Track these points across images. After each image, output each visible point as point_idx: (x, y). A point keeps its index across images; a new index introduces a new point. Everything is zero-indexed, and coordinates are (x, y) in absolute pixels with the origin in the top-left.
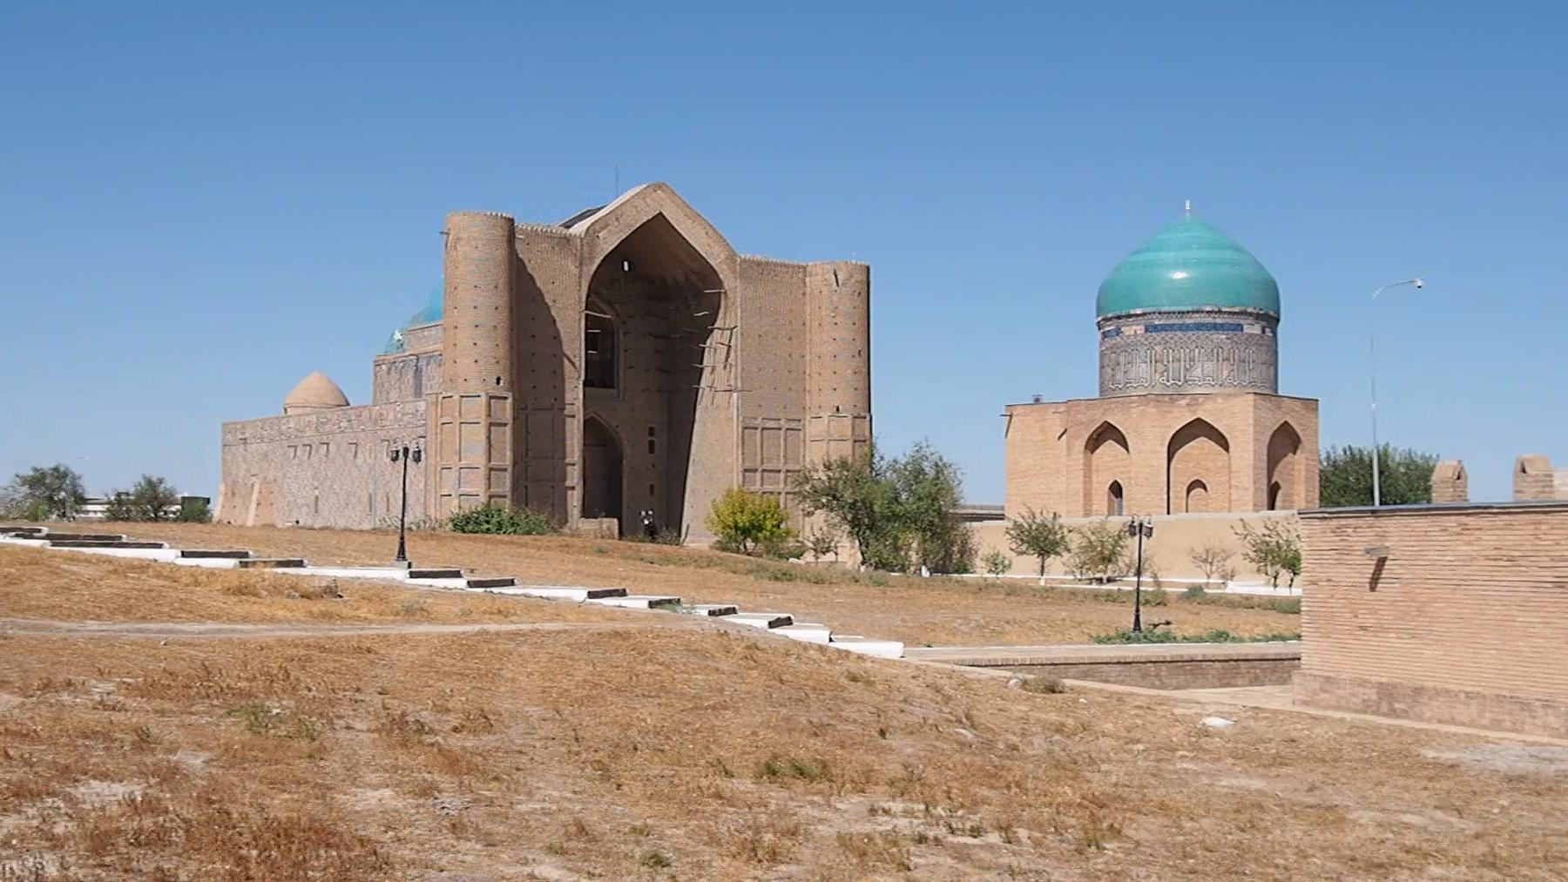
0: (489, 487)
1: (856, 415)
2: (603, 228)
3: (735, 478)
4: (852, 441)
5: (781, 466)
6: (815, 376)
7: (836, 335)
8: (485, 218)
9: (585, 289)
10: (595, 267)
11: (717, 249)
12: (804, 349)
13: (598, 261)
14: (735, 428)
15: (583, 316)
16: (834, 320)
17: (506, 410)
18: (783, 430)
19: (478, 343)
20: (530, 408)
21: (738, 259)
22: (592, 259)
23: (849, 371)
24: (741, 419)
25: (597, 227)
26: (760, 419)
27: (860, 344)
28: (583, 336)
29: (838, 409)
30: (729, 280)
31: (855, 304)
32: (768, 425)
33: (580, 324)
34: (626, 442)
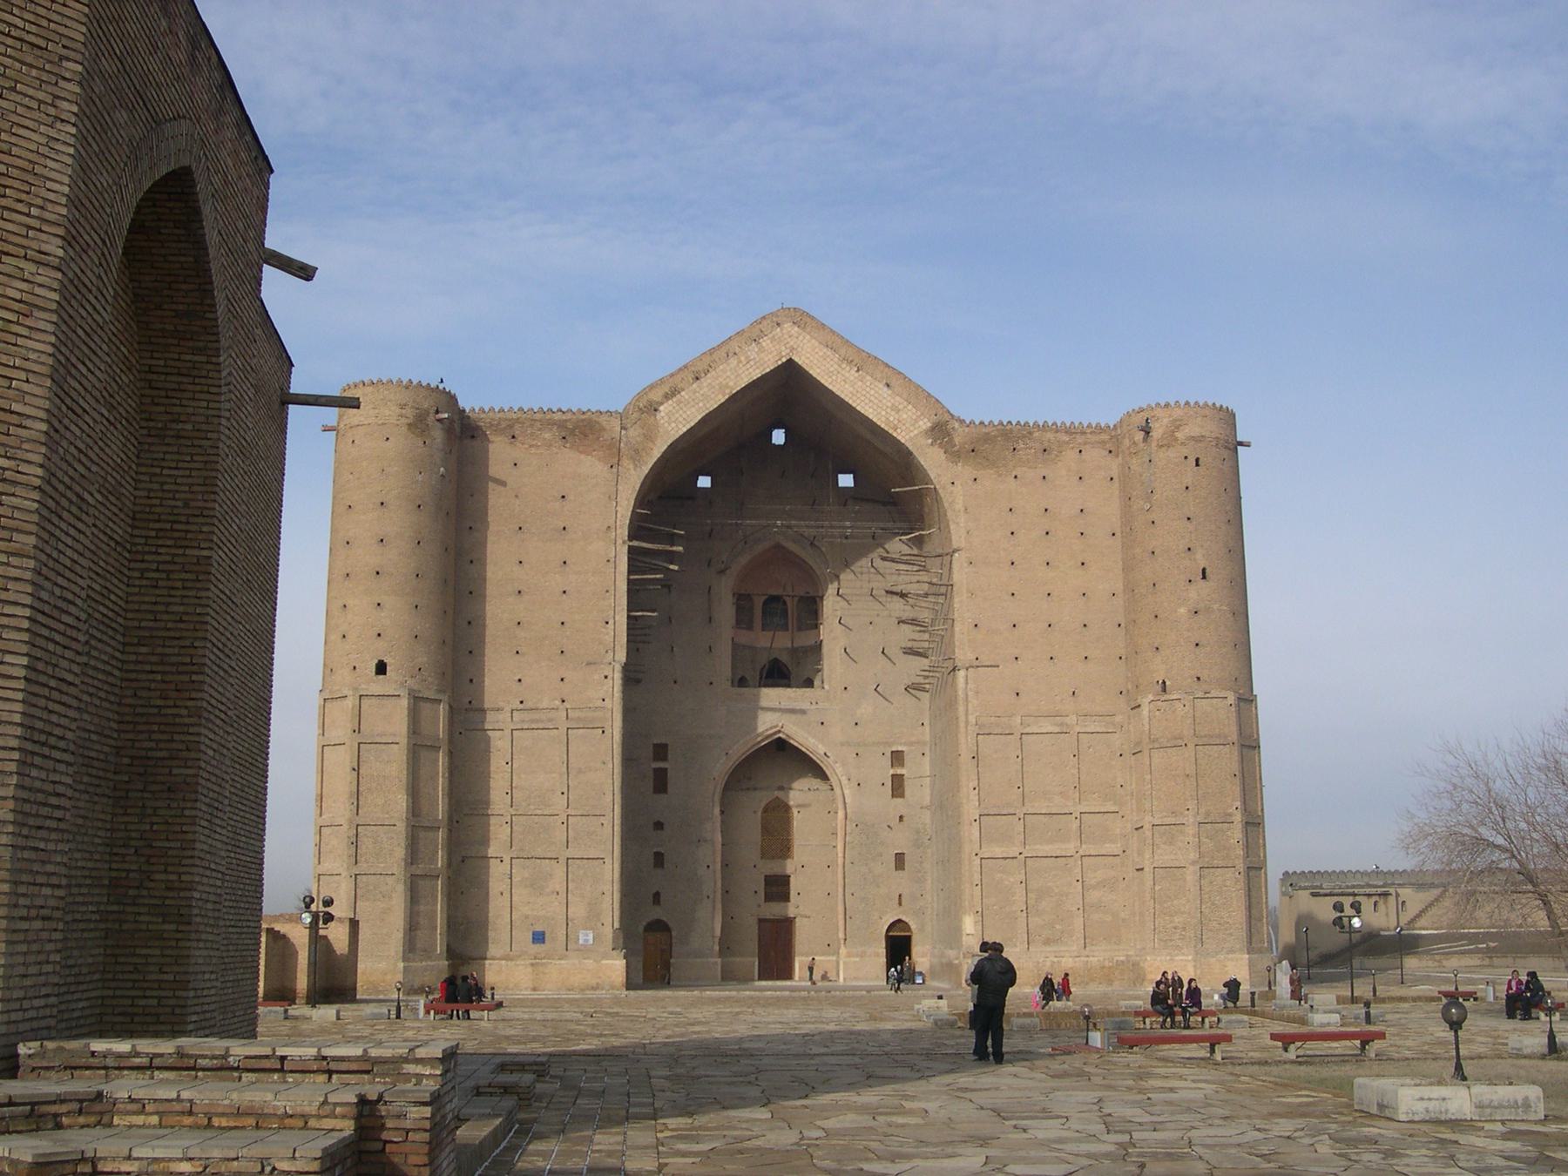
2: (667, 397)
11: (909, 413)
23: (1182, 610)
24: (972, 719)
28: (623, 587)
31: (1188, 481)
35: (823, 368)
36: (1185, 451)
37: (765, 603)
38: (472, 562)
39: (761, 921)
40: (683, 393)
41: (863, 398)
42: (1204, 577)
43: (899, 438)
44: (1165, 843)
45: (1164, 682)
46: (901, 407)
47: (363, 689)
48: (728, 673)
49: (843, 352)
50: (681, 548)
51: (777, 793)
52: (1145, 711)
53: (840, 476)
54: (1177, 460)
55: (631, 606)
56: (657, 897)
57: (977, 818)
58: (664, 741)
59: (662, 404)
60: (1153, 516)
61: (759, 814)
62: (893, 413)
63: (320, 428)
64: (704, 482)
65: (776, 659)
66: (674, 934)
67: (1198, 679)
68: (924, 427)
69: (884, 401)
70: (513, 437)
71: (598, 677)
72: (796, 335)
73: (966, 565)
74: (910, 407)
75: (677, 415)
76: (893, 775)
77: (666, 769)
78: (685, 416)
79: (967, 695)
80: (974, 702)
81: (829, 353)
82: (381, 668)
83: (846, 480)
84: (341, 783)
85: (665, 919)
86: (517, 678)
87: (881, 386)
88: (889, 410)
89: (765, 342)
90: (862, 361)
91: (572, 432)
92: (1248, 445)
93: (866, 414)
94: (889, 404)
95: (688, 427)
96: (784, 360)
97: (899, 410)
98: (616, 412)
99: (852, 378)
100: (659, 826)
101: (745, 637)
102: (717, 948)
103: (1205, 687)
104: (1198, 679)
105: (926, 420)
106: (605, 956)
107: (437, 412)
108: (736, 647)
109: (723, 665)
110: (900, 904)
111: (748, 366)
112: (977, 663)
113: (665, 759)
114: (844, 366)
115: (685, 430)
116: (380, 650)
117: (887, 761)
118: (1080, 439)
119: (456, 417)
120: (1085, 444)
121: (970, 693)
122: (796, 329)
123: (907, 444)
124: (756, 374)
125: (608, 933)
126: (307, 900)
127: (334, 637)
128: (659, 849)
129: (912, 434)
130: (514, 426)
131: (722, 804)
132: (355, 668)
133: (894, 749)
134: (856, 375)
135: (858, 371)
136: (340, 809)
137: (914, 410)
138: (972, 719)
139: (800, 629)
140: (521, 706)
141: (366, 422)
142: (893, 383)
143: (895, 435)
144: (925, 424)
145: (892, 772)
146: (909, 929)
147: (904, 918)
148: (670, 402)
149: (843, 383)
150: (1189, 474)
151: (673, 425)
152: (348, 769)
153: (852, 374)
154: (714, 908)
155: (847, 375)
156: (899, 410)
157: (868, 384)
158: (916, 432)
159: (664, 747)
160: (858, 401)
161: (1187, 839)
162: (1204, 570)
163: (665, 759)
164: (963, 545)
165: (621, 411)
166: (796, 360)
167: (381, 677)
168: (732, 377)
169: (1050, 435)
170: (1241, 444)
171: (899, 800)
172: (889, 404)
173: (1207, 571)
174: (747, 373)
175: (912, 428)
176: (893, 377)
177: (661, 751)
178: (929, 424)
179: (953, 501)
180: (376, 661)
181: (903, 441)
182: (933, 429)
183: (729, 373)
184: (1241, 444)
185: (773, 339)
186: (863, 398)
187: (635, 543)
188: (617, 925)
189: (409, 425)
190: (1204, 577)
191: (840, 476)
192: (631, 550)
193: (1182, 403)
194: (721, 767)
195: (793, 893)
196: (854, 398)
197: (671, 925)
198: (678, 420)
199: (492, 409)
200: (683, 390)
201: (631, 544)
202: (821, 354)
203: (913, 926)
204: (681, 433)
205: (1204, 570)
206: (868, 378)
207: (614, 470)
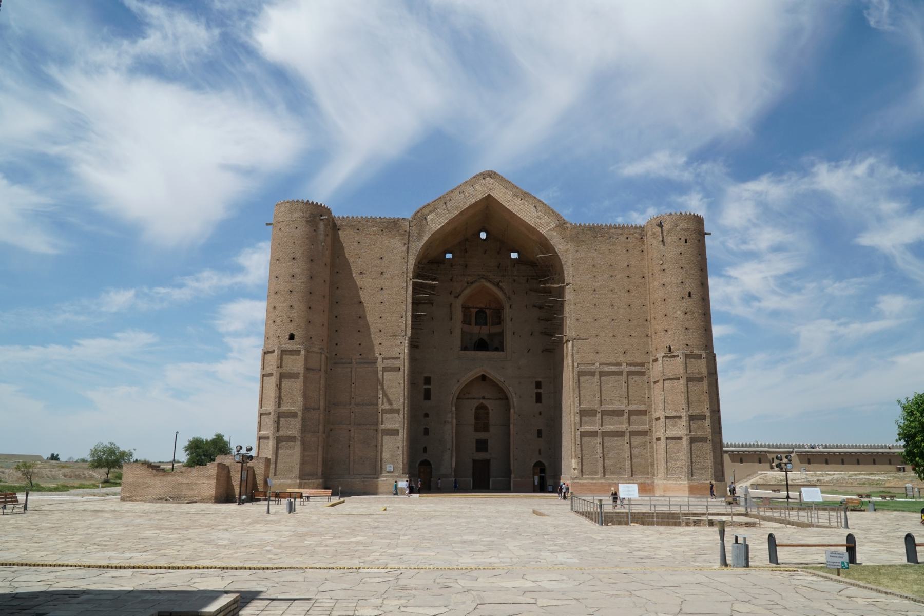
0: (278, 431)
1: (688, 352)
2: (431, 212)
3: (572, 419)
4: (685, 378)
5: (623, 407)
6: (653, 321)
7: (665, 280)
8: (288, 204)
9: (412, 261)
10: (423, 244)
12: (646, 299)
13: (425, 239)
14: (571, 374)
15: (411, 283)
16: (663, 267)
17: (297, 364)
18: (625, 374)
19: (277, 305)
21: (568, 225)
22: (420, 237)
24: (576, 364)
25: (426, 211)
26: (597, 364)
27: (691, 285)
28: (410, 300)
29: (670, 349)
30: (560, 246)
32: (607, 369)
33: (406, 291)
35: (505, 198)
36: (680, 236)
37: (477, 313)
38: (338, 288)
39: (474, 461)
40: (438, 210)
41: (523, 213)
42: (690, 296)
43: (541, 231)
44: (672, 425)
45: (670, 347)
46: (541, 217)
47: (283, 347)
48: (459, 343)
49: (514, 191)
50: (437, 282)
51: (482, 401)
52: (660, 360)
53: (512, 254)
54: (675, 240)
55: (414, 310)
56: (425, 449)
57: (578, 411)
58: (429, 375)
59: (428, 215)
60: (664, 267)
61: (474, 410)
62: (538, 220)
63: (265, 224)
64: (449, 256)
65: (481, 338)
66: (433, 466)
67: (687, 345)
68: (552, 226)
69: (533, 214)
70: (358, 230)
71: (398, 342)
72: (492, 183)
73: (572, 291)
74: (546, 217)
75: (436, 220)
76: (536, 393)
77: (430, 389)
78: (439, 220)
79: (573, 353)
80: (576, 356)
81: (507, 192)
82: (292, 337)
83: (514, 255)
84: (271, 392)
85: (428, 459)
86: (359, 343)
87: (532, 207)
88: (536, 218)
89: (478, 187)
91: (386, 228)
92: (709, 234)
93: (525, 220)
94: (536, 216)
95: (441, 226)
96: (486, 195)
97: (541, 218)
98: (407, 219)
99: (518, 203)
100: (426, 415)
102: (453, 474)
103: (691, 349)
104: (687, 345)
105: (553, 223)
106: (399, 477)
107: (321, 216)
109: (456, 339)
110: (540, 454)
111: (469, 197)
112: (577, 338)
113: (430, 384)
114: (514, 197)
115: (439, 227)
116: (291, 328)
117: (534, 384)
118: (626, 231)
119: (331, 220)
120: (630, 234)
121: (574, 352)
122: (492, 180)
123: (545, 234)
124: (473, 201)
125: (401, 465)
126: (239, 447)
127: (270, 322)
128: (427, 426)
129: (547, 230)
130: (358, 225)
131: (456, 405)
132: (279, 337)
133: (537, 380)
134: (520, 202)
135: (521, 200)
136: (270, 406)
137: (548, 218)
138: (576, 364)
139: (492, 325)
140: (360, 357)
141: (286, 219)
142: (538, 206)
143: (539, 230)
144: (553, 225)
145: (536, 391)
146: (544, 466)
147: (541, 460)
148: (432, 214)
149: (514, 206)
150: (683, 247)
151: (434, 225)
152: (275, 385)
153: (518, 201)
154: (452, 454)
155: (516, 202)
156: (541, 218)
157: (526, 206)
158: (548, 228)
159: (430, 378)
160: (521, 214)
161: (683, 423)
162: (690, 293)
163: (430, 384)
167: (292, 341)
168: (462, 203)
169: (613, 230)
171: (539, 405)
172: (536, 216)
173: (692, 293)
174: (469, 201)
175: (547, 227)
177: (428, 380)
178: (555, 225)
179: (567, 261)
180: (289, 333)
181: (542, 233)
182: (557, 226)
183: (460, 201)
184: (706, 234)
185: (481, 185)
186: (523, 213)
187: (415, 280)
188: (405, 462)
189: (307, 221)
190: (690, 296)
191: (512, 254)
192: (415, 285)
193: (678, 213)
194: (456, 389)
195: (489, 448)
196: (519, 213)
197: (431, 462)
198: (436, 222)
200: (438, 208)
201: (414, 280)
202: (504, 192)
203: (546, 464)
204: (437, 228)
205: (690, 293)
206: (526, 203)
207: (406, 246)
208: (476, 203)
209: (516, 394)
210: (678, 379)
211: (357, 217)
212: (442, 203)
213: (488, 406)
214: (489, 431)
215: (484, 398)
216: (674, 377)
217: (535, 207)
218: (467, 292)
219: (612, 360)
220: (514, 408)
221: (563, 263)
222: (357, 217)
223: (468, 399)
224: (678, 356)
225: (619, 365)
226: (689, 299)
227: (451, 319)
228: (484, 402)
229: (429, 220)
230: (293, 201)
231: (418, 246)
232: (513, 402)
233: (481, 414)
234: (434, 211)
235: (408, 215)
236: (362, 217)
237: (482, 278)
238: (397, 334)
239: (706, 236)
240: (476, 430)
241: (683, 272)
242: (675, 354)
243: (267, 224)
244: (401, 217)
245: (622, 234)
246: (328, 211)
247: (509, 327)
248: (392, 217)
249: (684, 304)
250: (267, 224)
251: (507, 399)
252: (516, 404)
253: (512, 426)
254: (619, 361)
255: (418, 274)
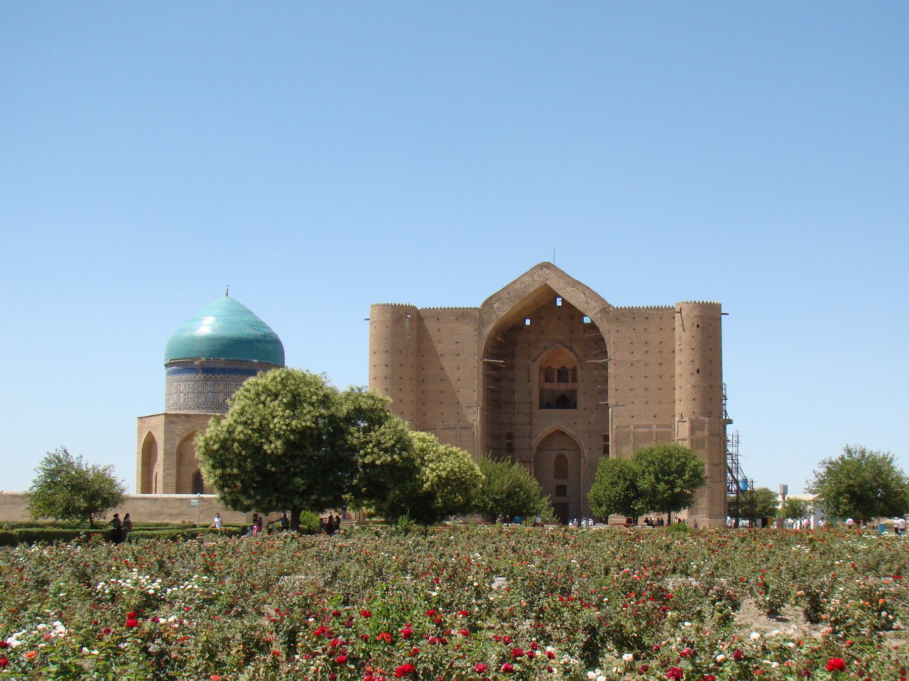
2: (497, 301)
10: (491, 329)
20: (438, 428)
21: (611, 309)
23: (689, 386)
24: (614, 427)
25: (493, 301)
26: (632, 427)
30: (603, 327)
34: (584, 447)
51: (562, 452)
90: (576, 284)
101: (548, 386)
108: (542, 391)
112: (616, 404)
117: (602, 438)
122: (548, 270)
130: (439, 314)
138: (614, 427)
145: (604, 443)
153: (569, 289)
162: (698, 370)
164: (613, 358)
165: (479, 307)
166: (548, 283)
169: (650, 312)
170: (723, 314)
173: (700, 370)
176: (586, 290)
177: (510, 436)
182: (601, 310)
184: (723, 314)
195: (567, 493)
198: (502, 311)
199: (430, 308)
208: (535, 291)
209: (586, 446)
210: (685, 440)
211: (437, 308)
212: (506, 293)
213: (567, 455)
214: (567, 478)
215: (563, 449)
216: (684, 438)
217: (584, 294)
218: (544, 355)
219: (644, 423)
220: (584, 458)
221: (606, 341)
222: (437, 308)
223: (549, 450)
224: (686, 421)
225: (650, 427)
226: (696, 375)
227: (529, 381)
228: (562, 452)
229: (495, 308)
230: (384, 304)
231: (488, 330)
232: (584, 453)
233: (561, 461)
234: (499, 300)
235: (479, 305)
236: (441, 308)
237: (557, 342)
238: (471, 405)
239: (722, 316)
240: (556, 477)
241: (694, 353)
242: (685, 419)
243: (366, 320)
244: (473, 307)
245: (657, 315)
246: (414, 308)
247: (580, 387)
248: (465, 307)
249: (693, 379)
250: (366, 320)
251: (578, 449)
252: (586, 455)
253: (582, 474)
254: (650, 423)
255: (488, 354)
